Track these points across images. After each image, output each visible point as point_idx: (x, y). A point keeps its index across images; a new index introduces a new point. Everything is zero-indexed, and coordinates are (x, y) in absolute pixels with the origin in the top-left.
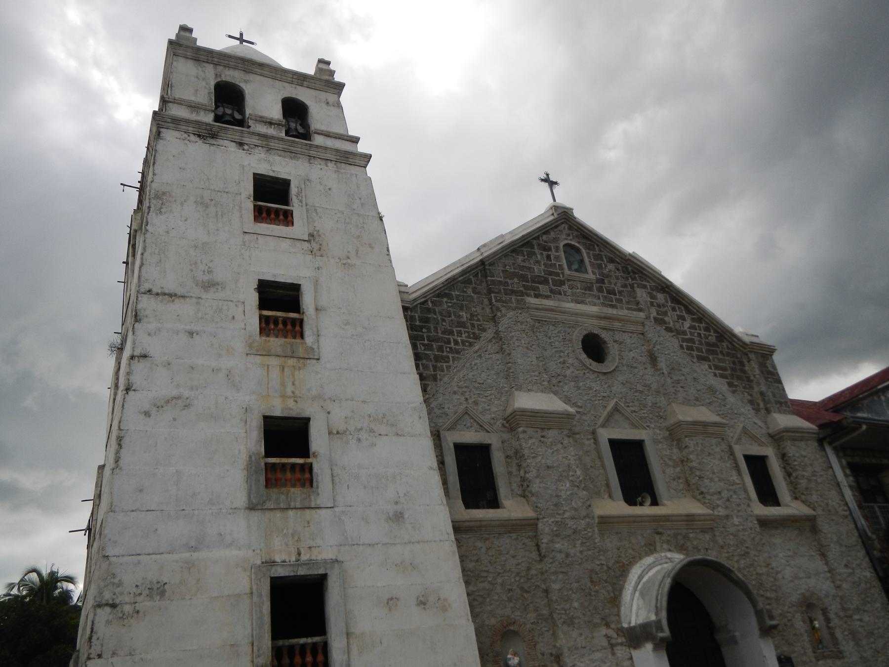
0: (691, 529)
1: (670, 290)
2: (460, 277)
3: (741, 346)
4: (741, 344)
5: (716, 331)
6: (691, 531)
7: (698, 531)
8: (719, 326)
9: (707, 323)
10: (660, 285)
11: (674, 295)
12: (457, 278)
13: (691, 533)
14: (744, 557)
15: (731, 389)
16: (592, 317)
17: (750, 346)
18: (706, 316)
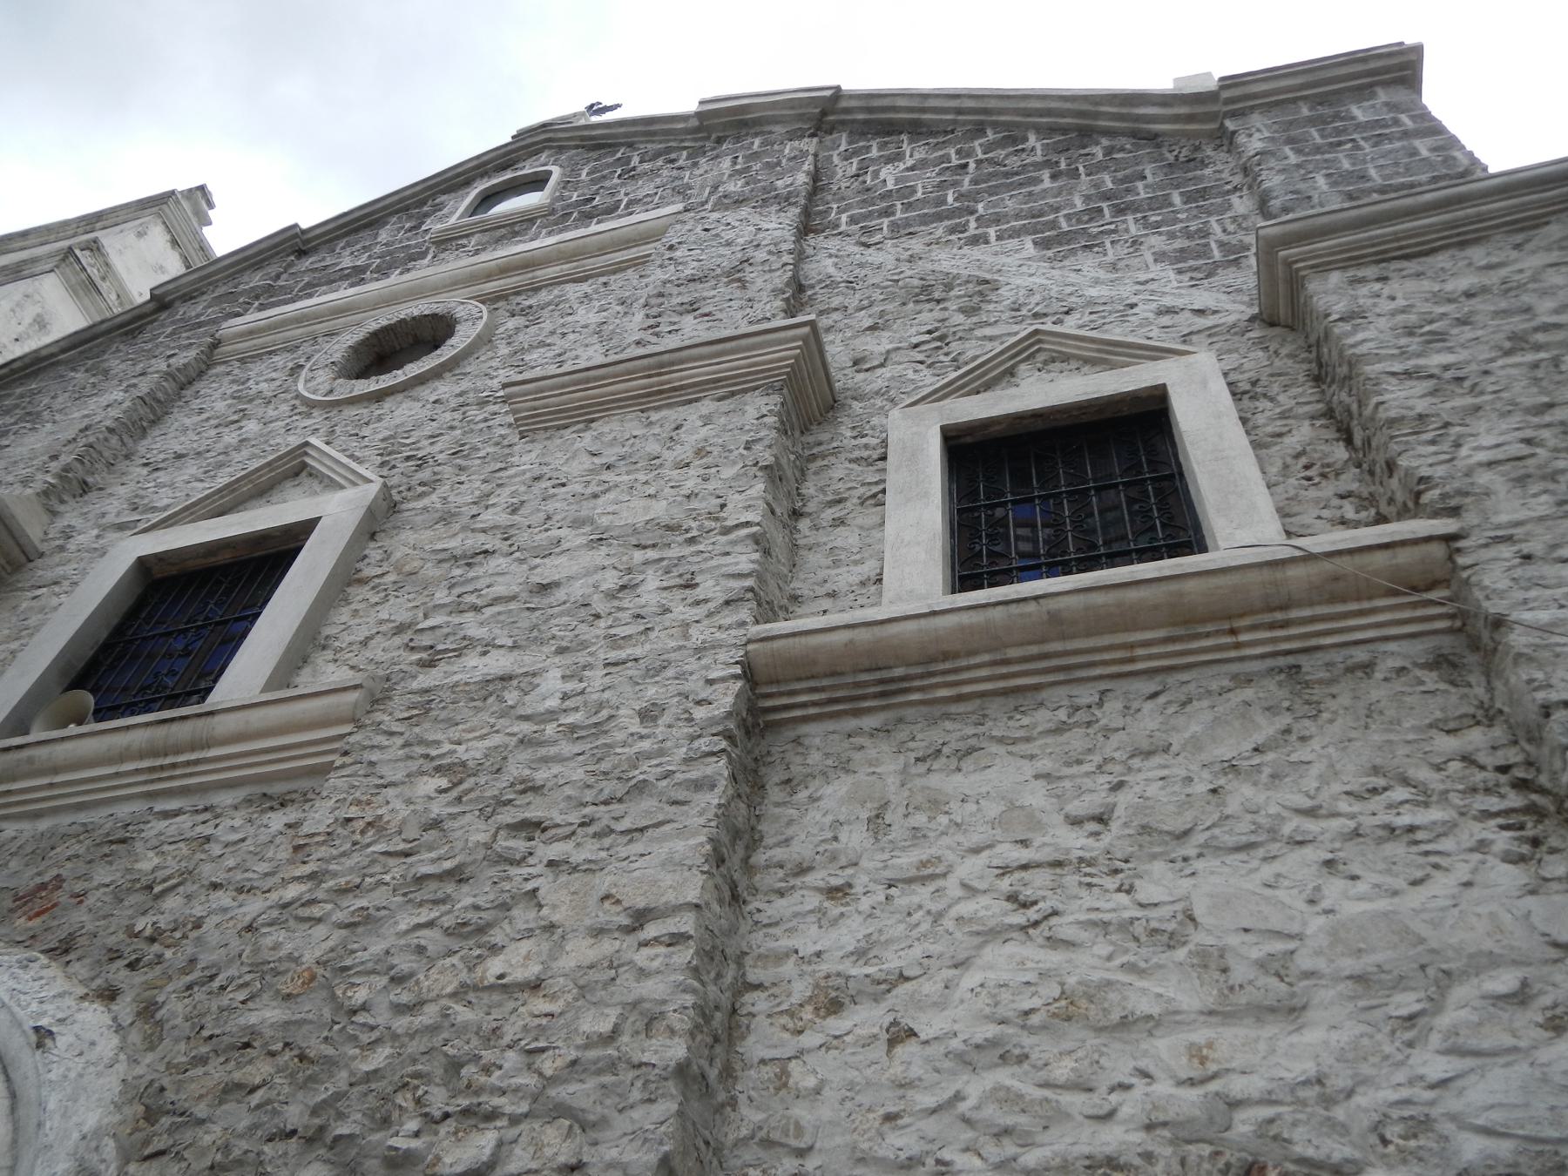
0: (185, 791)
1: (847, 111)
2: (63, 351)
3: (1190, 118)
4: (1184, 110)
5: (1045, 131)
6: (173, 805)
7: (224, 799)
8: (1054, 105)
9: (1007, 126)
10: (800, 118)
11: (861, 116)
12: (53, 355)
13: (166, 815)
14: (450, 888)
15: (1050, 253)
16: (455, 283)
17: (1225, 94)
18: (992, 104)
